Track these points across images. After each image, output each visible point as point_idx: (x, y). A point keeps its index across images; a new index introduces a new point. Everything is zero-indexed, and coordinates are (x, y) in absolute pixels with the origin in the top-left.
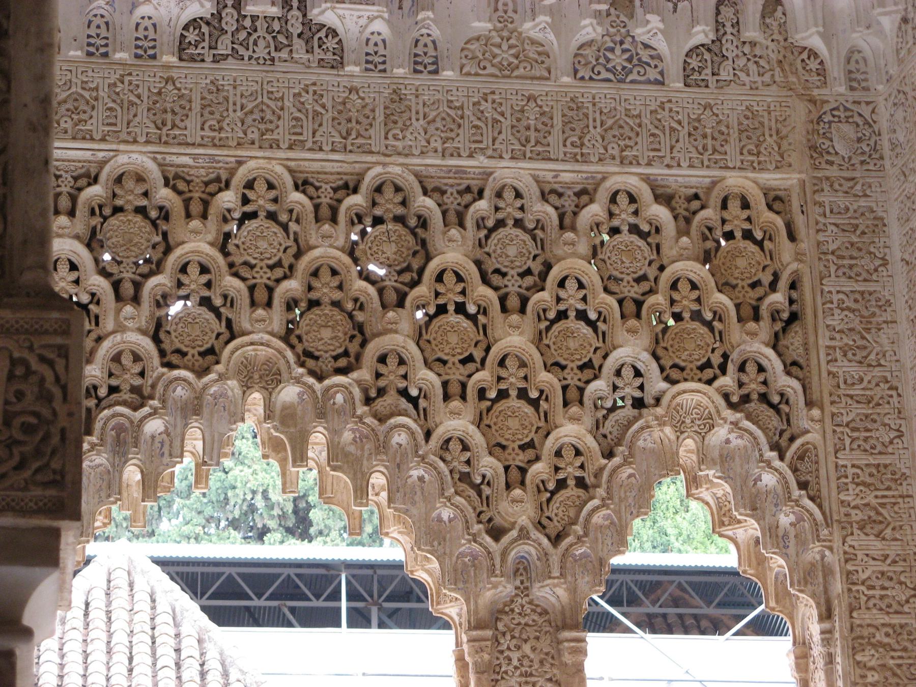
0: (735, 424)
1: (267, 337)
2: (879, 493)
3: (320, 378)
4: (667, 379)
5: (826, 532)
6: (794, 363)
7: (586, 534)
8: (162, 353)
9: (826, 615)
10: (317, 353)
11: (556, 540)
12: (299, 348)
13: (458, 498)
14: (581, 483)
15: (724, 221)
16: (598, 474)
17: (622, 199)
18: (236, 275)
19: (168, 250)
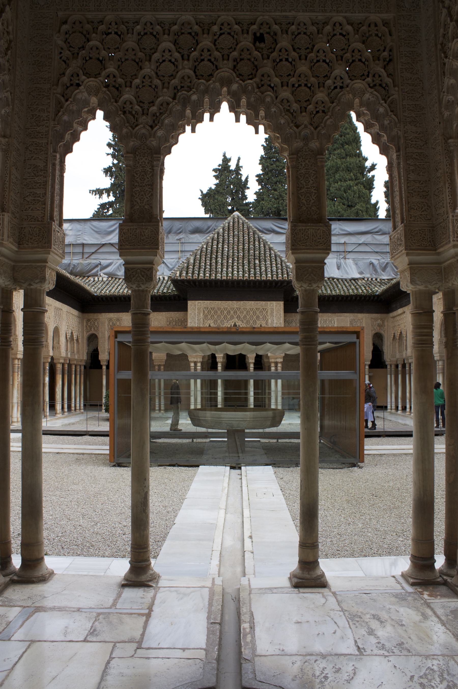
0: (371, 93)
1: (227, 69)
2: (416, 113)
3: (244, 81)
4: (351, 79)
5: (399, 125)
6: (390, 74)
7: (325, 126)
8: (196, 76)
9: (398, 150)
10: (243, 74)
11: (316, 128)
12: (238, 73)
13: (286, 116)
14: (323, 112)
15: (369, 31)
16: (329, 109)
17: (337, 25)
18: (219, 51)
19: (198, 44)
